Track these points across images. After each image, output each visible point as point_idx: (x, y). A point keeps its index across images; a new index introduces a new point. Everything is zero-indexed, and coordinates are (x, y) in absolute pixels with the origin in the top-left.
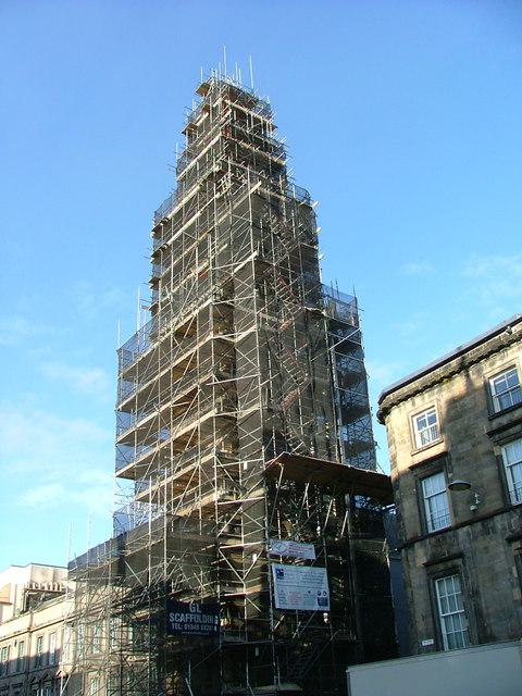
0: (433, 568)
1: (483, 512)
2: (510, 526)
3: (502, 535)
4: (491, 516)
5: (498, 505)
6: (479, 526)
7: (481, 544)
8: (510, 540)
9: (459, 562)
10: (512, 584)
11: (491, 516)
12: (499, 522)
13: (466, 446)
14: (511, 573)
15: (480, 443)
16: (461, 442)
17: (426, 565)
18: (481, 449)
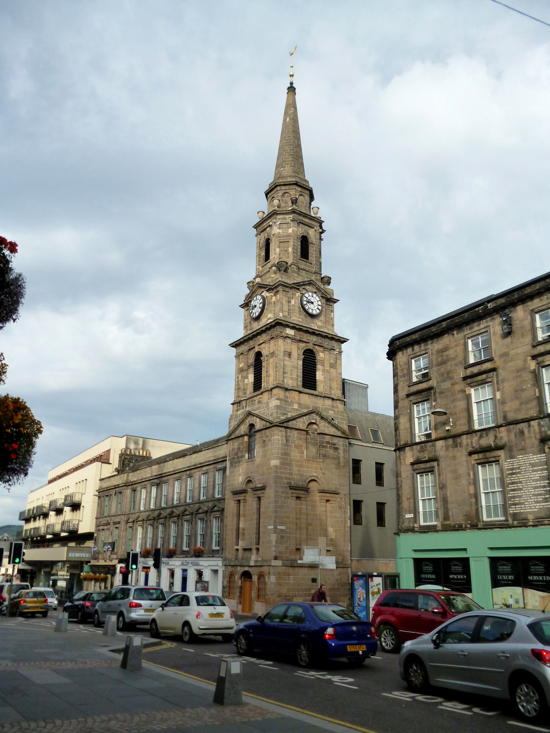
0: (415, 466)
1: (454, 432)
2: (472, 443)
3: (466, 449)
4: (460, 435)
5: (465, 428)
6: (450, 441)
7: (452, 452)
8: (470, 454)
9: (435, 464)
10: (469, 483)
11: (460, 435)
12: (464, 439)
13: (447, 385)
14: (469, 475)
15: (457, 383)
16: (444, 381)
17: (412, 464)
18: (458, 387)
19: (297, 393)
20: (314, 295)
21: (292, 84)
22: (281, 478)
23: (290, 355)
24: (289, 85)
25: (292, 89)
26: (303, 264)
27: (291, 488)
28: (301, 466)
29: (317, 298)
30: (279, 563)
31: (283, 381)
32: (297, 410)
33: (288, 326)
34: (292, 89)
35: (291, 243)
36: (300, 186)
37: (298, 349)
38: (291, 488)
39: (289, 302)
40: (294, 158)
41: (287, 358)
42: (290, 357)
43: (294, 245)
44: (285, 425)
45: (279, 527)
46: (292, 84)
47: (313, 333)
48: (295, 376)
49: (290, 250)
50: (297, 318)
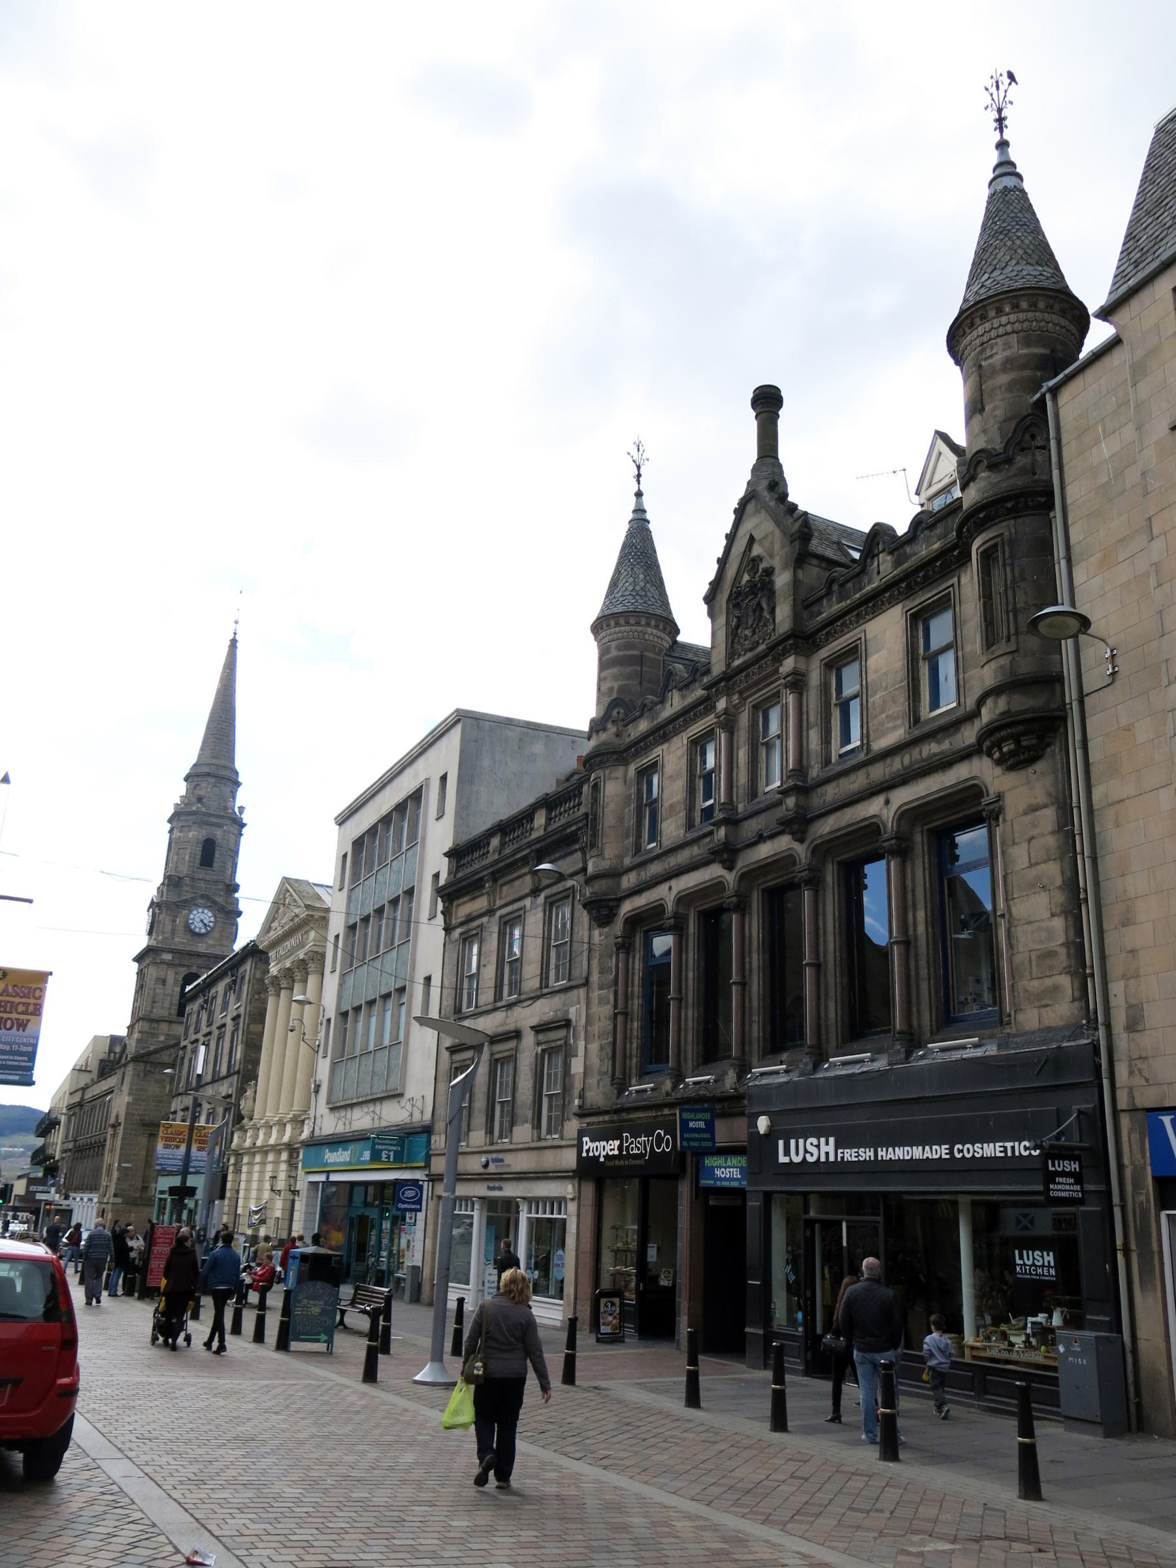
19: (167, 1024)
20: (206, 911)
21: (235, 634)
22: (133, 1115)
23: (164, 982)
24: (232, 636)
25: (234, 643)
26: (202, 874)
27: (144, 1125)
28: (160, 1102)
29: (210, 914)
30: (119, 1200)
31: (151, 1012)
32: (164, 1042)
33: (163, 951)
34: (234, 643)
35: (189, 851)
36: (214, 776)
37: (176, 973)
38: (144, 1125)
39: (174, 921)
40: (218, 739)
41: (161, 986)
42: (164, 985)
43: (191, 853)
44: (145, 1059)
45: (123, 1165)
46: (235, 634)
47: (199, 955)
48: (167, 1004)
49: (187, 858)
50: (181, 941)
